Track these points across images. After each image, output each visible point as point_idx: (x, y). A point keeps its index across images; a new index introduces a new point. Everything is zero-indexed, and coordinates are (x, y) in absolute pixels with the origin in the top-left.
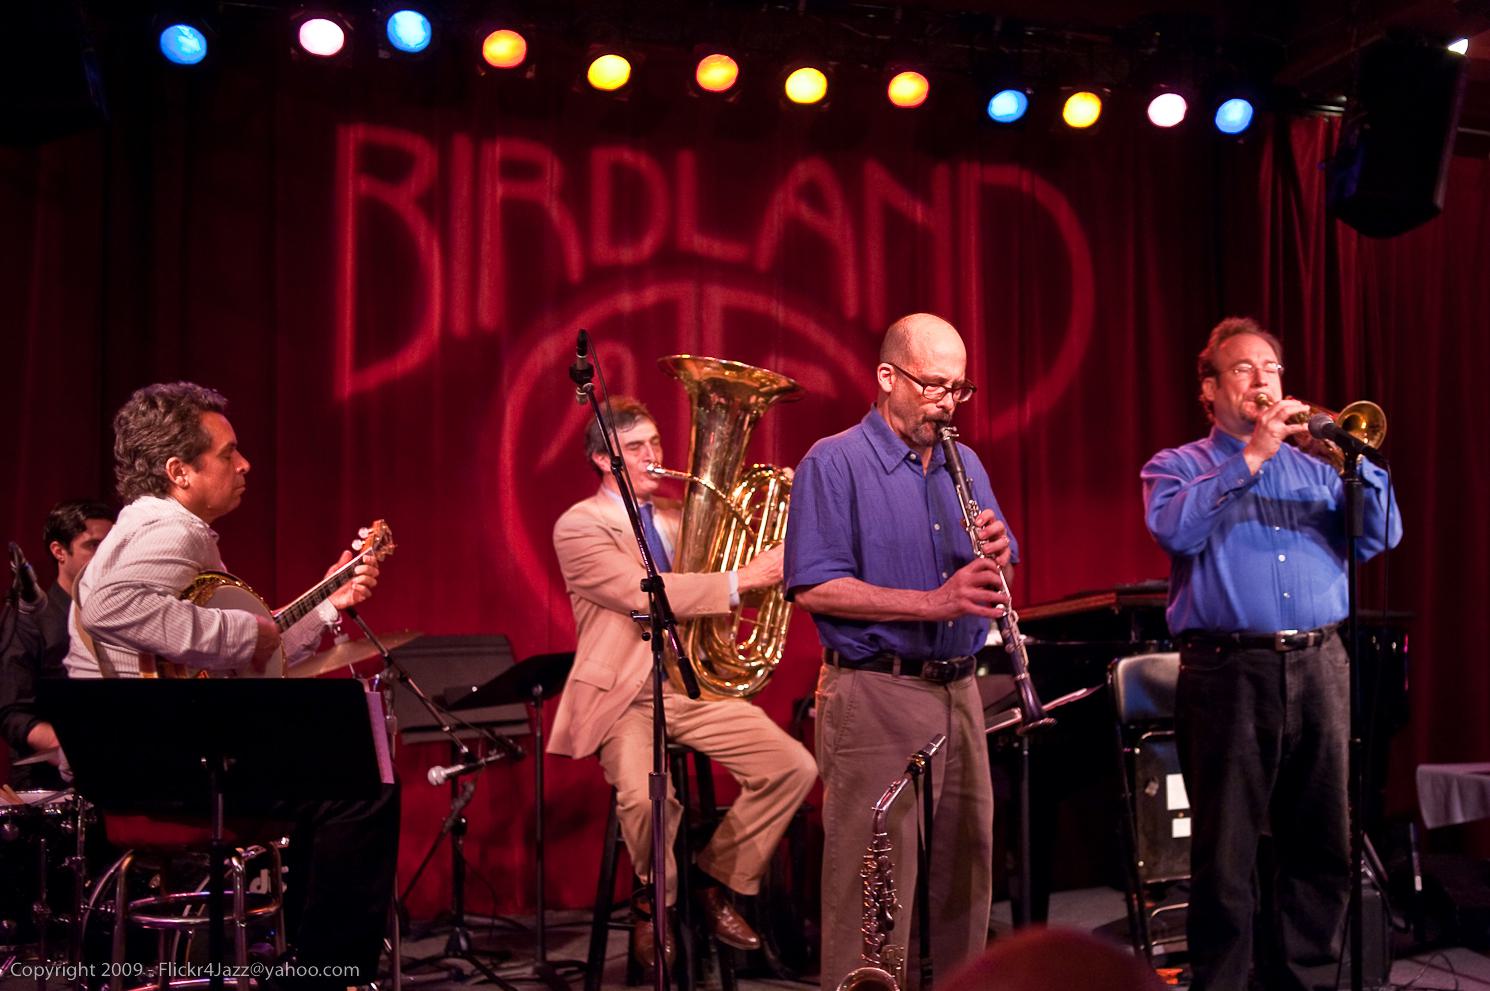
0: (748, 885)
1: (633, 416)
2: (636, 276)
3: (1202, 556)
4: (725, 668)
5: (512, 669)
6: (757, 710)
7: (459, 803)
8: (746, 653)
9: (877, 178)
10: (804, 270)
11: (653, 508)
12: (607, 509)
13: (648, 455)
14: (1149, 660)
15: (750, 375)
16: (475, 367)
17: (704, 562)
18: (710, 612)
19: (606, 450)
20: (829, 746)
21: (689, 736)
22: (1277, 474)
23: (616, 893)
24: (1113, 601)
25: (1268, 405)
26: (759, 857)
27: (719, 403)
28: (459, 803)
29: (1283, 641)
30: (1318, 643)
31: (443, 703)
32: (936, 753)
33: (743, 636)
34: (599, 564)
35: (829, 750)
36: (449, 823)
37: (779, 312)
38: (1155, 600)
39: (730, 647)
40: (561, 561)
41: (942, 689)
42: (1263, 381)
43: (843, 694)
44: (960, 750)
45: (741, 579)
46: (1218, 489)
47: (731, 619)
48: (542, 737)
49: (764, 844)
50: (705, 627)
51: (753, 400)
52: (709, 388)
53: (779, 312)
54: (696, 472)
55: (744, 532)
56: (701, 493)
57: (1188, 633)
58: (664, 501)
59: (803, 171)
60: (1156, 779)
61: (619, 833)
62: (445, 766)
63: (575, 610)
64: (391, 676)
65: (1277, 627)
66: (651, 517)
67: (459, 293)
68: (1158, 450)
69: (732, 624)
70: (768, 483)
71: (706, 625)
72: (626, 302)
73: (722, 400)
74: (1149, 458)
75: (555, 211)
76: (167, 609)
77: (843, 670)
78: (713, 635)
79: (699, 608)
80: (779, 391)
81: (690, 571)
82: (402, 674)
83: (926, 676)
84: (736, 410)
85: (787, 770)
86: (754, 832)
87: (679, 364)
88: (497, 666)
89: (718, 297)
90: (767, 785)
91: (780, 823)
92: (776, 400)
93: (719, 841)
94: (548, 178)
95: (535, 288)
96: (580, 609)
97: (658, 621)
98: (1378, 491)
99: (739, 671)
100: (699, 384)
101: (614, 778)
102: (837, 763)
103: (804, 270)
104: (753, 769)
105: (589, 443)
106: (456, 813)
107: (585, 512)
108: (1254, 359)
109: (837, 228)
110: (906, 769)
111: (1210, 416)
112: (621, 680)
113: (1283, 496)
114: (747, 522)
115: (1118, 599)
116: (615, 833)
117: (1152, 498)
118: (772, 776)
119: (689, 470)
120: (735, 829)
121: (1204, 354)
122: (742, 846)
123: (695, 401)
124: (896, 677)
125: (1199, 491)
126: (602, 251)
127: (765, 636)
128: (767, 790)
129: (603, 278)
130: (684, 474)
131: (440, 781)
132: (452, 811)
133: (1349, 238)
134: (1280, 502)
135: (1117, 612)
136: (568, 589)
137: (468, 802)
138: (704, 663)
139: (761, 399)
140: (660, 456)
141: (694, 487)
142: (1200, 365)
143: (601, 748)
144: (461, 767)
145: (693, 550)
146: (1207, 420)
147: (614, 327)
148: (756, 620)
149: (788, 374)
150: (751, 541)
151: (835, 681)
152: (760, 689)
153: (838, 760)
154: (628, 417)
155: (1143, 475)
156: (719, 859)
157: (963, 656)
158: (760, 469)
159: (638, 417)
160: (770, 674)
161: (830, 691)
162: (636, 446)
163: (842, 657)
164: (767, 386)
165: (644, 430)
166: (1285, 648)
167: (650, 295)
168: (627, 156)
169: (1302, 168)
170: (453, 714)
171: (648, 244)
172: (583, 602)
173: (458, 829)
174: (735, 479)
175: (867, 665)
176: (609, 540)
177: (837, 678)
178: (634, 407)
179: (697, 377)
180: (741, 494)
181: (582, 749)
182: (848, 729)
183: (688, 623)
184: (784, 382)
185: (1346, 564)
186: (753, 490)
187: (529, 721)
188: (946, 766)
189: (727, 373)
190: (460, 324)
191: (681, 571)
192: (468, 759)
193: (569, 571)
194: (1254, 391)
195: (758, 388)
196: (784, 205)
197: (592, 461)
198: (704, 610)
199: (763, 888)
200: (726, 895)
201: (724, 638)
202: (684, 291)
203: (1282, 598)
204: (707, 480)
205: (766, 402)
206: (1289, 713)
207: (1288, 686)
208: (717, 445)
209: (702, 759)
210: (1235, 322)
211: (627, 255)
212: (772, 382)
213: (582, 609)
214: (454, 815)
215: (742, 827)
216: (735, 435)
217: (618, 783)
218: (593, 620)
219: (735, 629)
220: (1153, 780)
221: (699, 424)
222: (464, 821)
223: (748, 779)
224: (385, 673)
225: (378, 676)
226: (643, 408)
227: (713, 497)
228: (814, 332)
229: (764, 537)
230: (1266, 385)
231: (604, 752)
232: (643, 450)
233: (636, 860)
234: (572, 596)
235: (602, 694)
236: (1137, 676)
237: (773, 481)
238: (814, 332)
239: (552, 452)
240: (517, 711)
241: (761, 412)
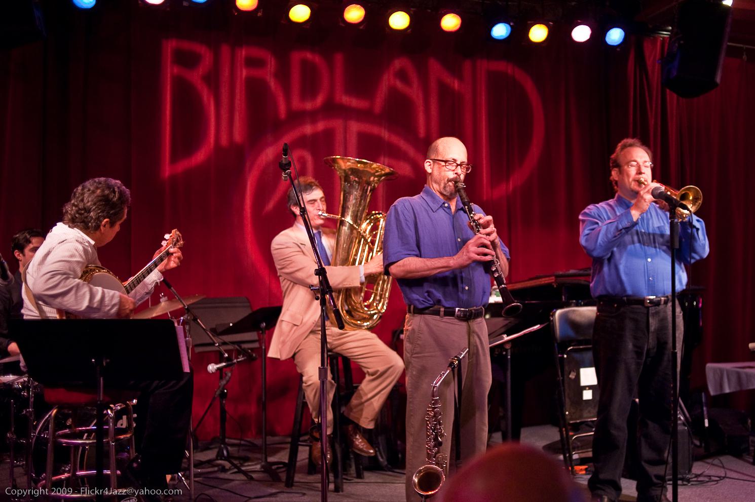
0: (369, 424)
1: (311, 187)
2: (313, 116)
3: (609, 260)
4: (357, 314)
5: (250, 314)
6: (374, 335)
7: (223, 382)
8: (368, 307)
9: (435, 66)
10: (399, 114)
11: (322, 233)
12: (297, 234)
13: (319, 207)
14: (571, 310)
15: (370, 166)
16: (232, 162)
17: (347, 261)
18: (350, 286)
19: (298, 204)
20: (409, 353)
21: (339, 348)
22: (648, 220)
23: (303, 428)
24: (553, 281)
25: (644, 184)
26: (374, 410)
27: (355, 180)
28: (223, 382)
29: (648, 301)
30: (666, 303)
31: (214, 331)
32: (464, 357)
33: (367, 298)
34: (293, 262)
35: (408, 355)
36: (218, 393)
37: (385, 134)
38: (582, 281)
39: (360, 303)
40: (275, 260)
41: (464, 324)
42: (643, 171)
44: (474, 354)
45: (365, 269)
46: (617, 227)
47: (361, 290)
48: (265, 349)
49: (377, 403)
50: (348, 293)
51: (372, 179)
52: (350, 173)
53: (385, 134)
54: (343, 215)
55: (367, 245)
56: (346, 226)
57: (600, 297)
58: (327, 230)
59: (397, 64)
60: (575, 370)
61: (304, 397)
62: (216, 363)
63: (282, 285)
64: (189, 318)
65: (645, 294)
66: (321, 238)
67: (224, 124)
68: (588, 205)
69: (361, 292)
70: (379, 221)
71: (348, 292)
72: (308, 129)
73: (357, 179)
74: (584, 209)
75: (272, 83)
76: (78, 286)
78: (351, 297)
79: (345, 283)
80: (386, 174)
81: (340, 265)
82: (194, 317)
83: (457, 317)
84: (363, 184)
85: (389, 366)
86: (372, 397)
87: (334, 161)
88: (242, 313)
89: (355, 127)
90: (379, 373)
91: (385, 393)
92: (384, 179)
93: (354, 401)
94: (269, 66)
95: (262, 122)
96: (284, 284)
97: (323, 290)
98: (698, 229)
99: (365, 316)
100: (345, 170)
101: (301, 369)
102: (412, 361)
103: (399, 114)
104: (371, 365)
105: (289, 200)
106: (222, 386)
107: (287, 235)
108: (639, 160)
109: (415, 92)
110: (448, 365)
111: (616, 187)
112: (304, 321)
113: (651, 231)
114: (369, 240)
115: (556, 280)
116: (302, 398)
117: (584, 229)
118: (381, 369)
119: (340, 214)
120: (362, 395)
121: (613, 156)
122: (366, 404)
123: (343, 179)
124: (442, 317)
125: (607, 227)
126: (296, 104)
127: (378, 298)
128: (379, 376)
129: (297, 117)
130: (337, 216)
131: (214, 371)
132: (220, 387)
133: (672, 98)
134: (649, 234)
135: (555, 286)
136: (278, 274)
137: (228, 382)
138: (347, 311)
139: (376, 179)
140: (325, 208)
141: (342, 223)
142: (611, 162)
143: (295, 354)
144: (224, 364)
145: (342, 254)
146: (614, 189)
147: (302, 142)
148: (373, 290)
149: (390, 166)
150: (371, 250)
152: (375, 325)
153: (413, 360)
154: (309, 187)
155: (580, 217)
156: (354, 410)
158: (376, 214)
159: (314, 187)
160: (381, 317)
162: (313, 202)
164: (378, 172)
165: (317, 194)
166: (649, 305)
167: (321, 126)
168: (309, 56)
169: (649, 62)
170: (220, 337)
171: (320, 100)
172: (286, 281)
173: (223, 395)
174: (363, 219)
176: (299, 249)
178: (312, 182)
179: (344, 168)
180: (366, 227)
181: (284, 356)
182: (418, 344)
183: (339, 291)
184: (387, 170)
185: (683, 266)
186: (372, 224)
187: (259, 341)
188: (469, 363)
189: (359, 165)
190: (224, 141)
191: (336, 265)
192: (229, 359)
193: (279, 265)
194: (637, 176)
195: (374, 173)
196: (388, 81)
197: (291, 209)
198: (347, 285)
199: (376, 425)
200: (358, 428)
201: (358, 299)
202: (337, 124)
203: (649, 280)
204: (348, 219)
205: (379, 180)
206: (650, 338)
207: (650, 325)
208: (354, 201)
209: (346, 360)
210: (630, 141)
211: (309, 106)
212: (382, 170)
213: (285, 284)
214: (221, 389)
215: (366, 394)
216: (363, 196)
217: (303, 372)
218: (291, 290)
219: (363, 294)
220: (574, 371)
221: (344, 191)
222: (226, 391)
223: (369, 370)
224: (186, 316)
225: (182, 318)
226: (316, 183)
227: (352, 228)
228: (404, 145)
229: (377, 248)
230: (644, 173)
231: (296, 357)
232: (316, 204)
233: (312, 411)
234: (280, 278)
235: (295, 327)
236: (565, 318)
237: (382, 220)
238: (404, 145)
239: (271, 205)
240: (253, 335)
241: (376, 185)
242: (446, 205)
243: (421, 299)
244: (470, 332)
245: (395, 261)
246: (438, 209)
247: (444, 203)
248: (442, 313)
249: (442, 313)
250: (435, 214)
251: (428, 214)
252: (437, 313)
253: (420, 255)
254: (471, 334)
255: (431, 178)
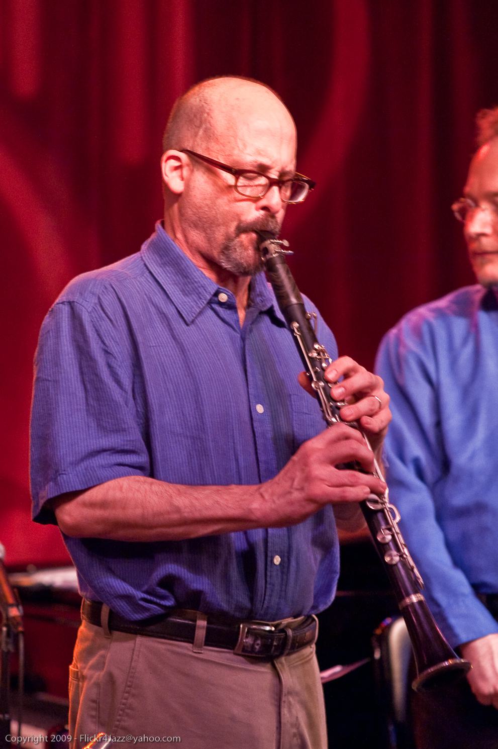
41: (265, 670)
43: (116, 673)
77: (116, 634)
124: (200, 647)
151: (102, 652)
157: (295, 617)
161: (95, 667)
163: (112, 614)
175: (152, 628)
177: (105, 647)
242: (223, 297)
243: (139, 594)
244: (279, 695)
245: (79, 488)
246: (201, 313)
247: (217, 294)
248: (201, 634)
249: (201, 634)
250: (192, 327)
251: (171, 329)
252: (187, 634)
253: (150, 471)
254: (284, 699)
255: (181, 214)
